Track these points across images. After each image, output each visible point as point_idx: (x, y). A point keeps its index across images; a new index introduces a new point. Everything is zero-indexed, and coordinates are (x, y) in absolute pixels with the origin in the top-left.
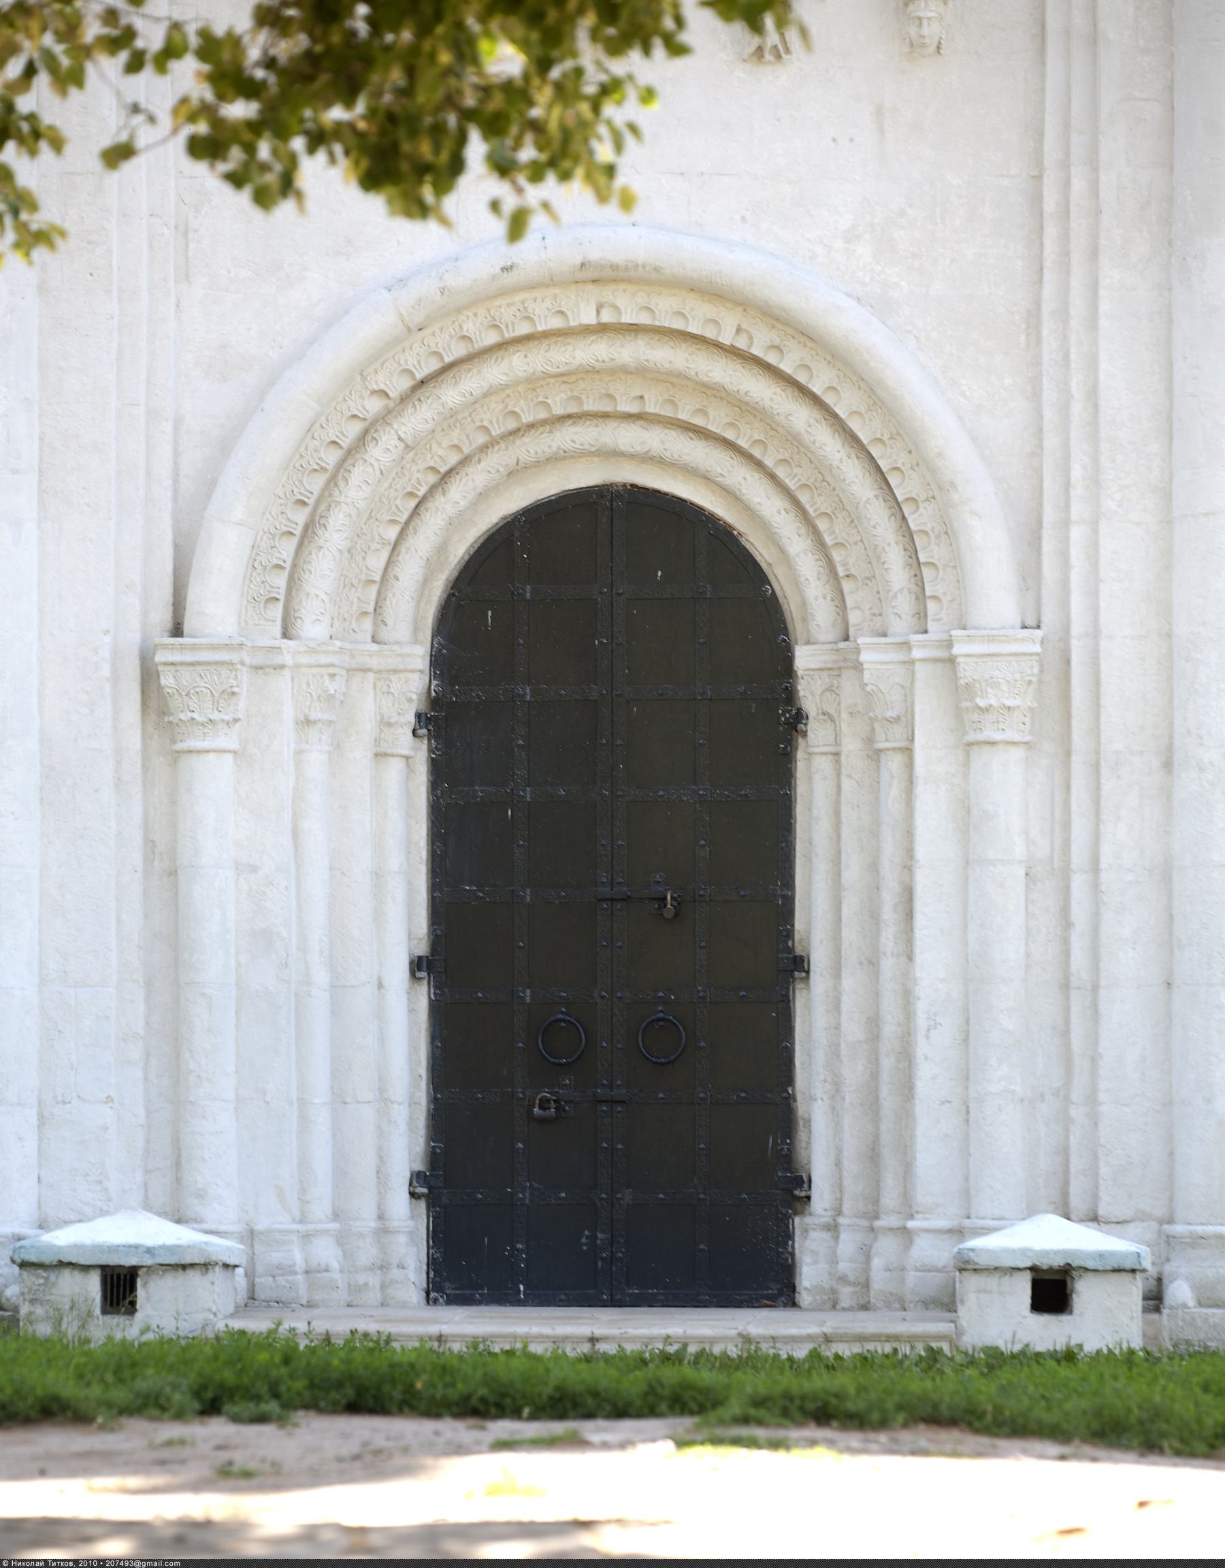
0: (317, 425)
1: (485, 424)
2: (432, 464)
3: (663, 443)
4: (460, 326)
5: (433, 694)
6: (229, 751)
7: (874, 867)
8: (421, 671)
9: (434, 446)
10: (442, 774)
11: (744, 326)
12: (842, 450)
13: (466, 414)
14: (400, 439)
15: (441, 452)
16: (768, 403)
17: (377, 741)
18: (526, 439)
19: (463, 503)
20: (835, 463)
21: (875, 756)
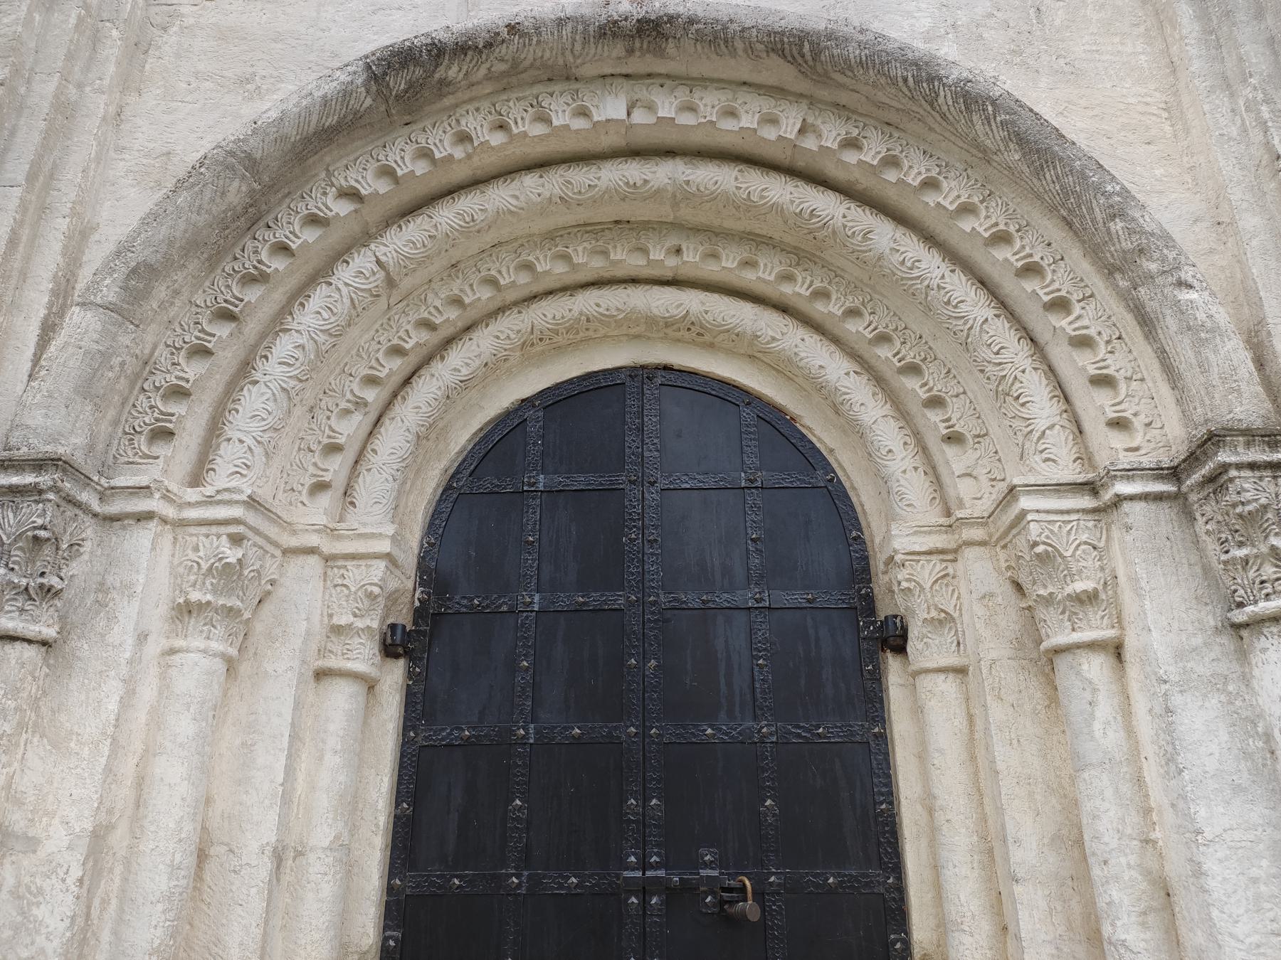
0: (262, 223)
1: (493, 272)
2: (426, 315)
3: (703, 304)
4: (458, 121)
5: (417, 604)
6: (29, 641)
7: (1073, 842)
8: (388, 556)
9: (430, 296)
10: (418, 708)
11: (810, 120)
12: (943, 266)
13: (472, 262)
14: (378, 262)
15: (438, 303)
16: (839, 221)
17: (322, 652)
18: (544, 303)
19: (465, 371)
20: (934, 283)
21: (1047, 662)
